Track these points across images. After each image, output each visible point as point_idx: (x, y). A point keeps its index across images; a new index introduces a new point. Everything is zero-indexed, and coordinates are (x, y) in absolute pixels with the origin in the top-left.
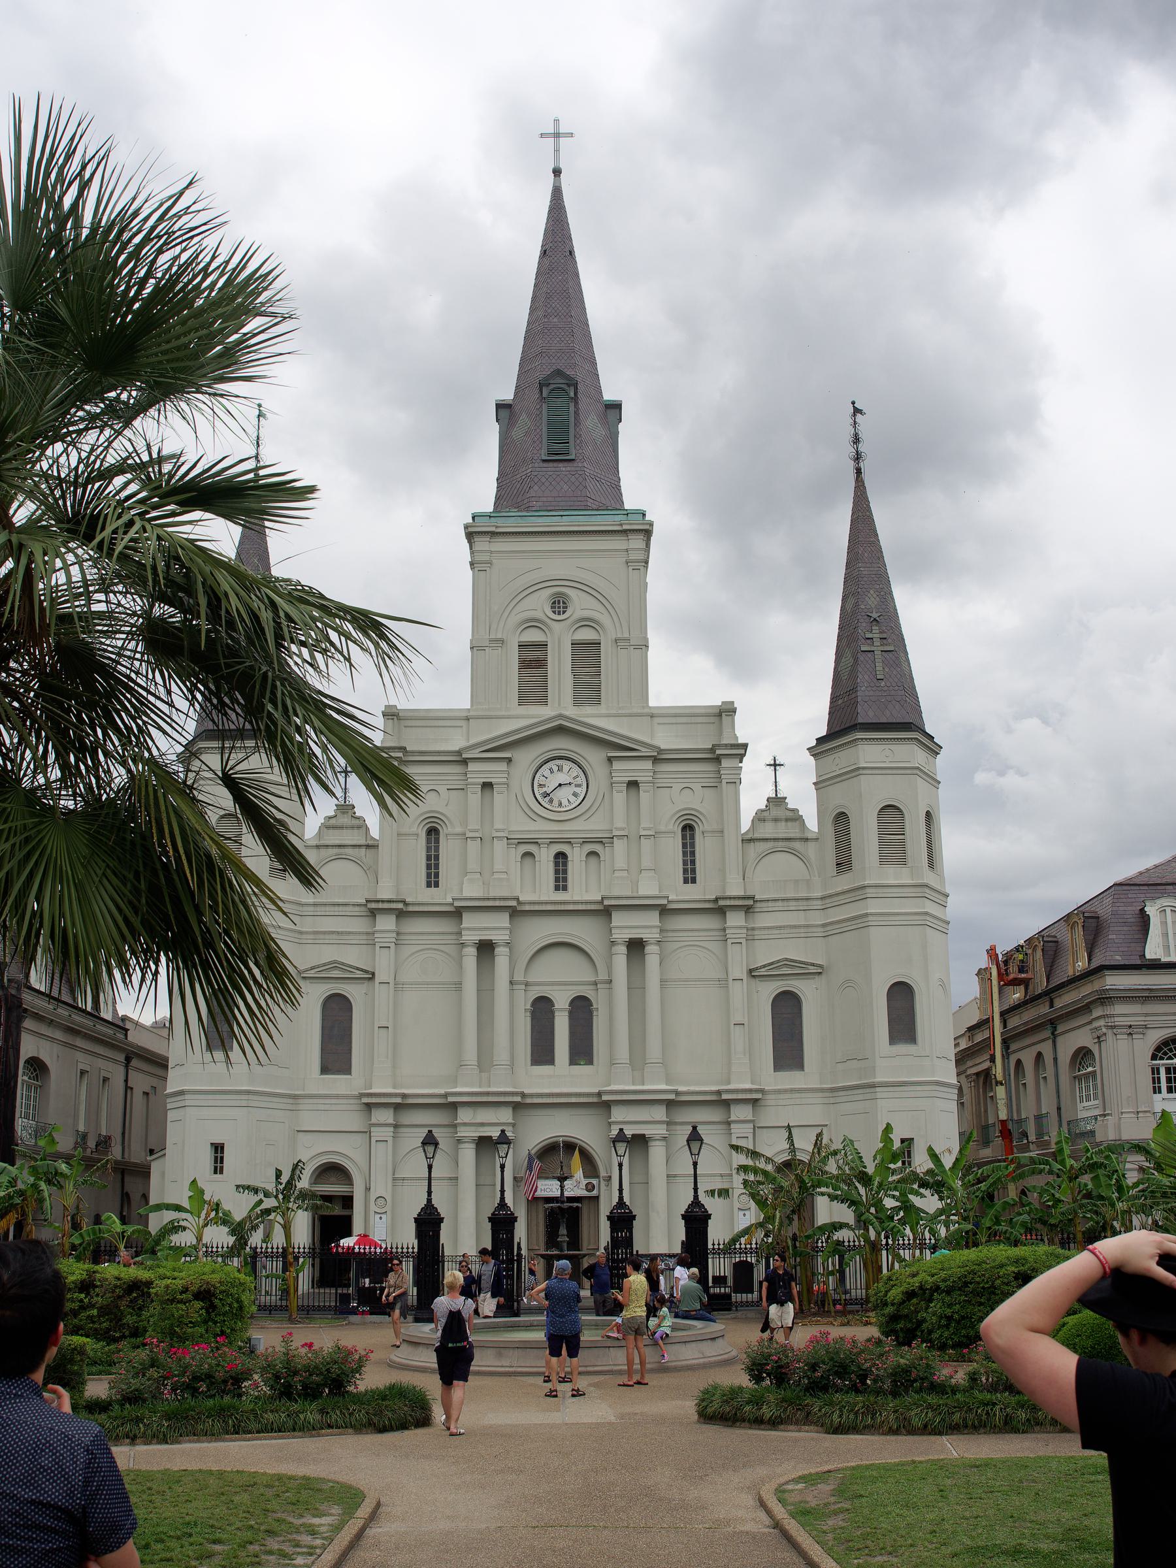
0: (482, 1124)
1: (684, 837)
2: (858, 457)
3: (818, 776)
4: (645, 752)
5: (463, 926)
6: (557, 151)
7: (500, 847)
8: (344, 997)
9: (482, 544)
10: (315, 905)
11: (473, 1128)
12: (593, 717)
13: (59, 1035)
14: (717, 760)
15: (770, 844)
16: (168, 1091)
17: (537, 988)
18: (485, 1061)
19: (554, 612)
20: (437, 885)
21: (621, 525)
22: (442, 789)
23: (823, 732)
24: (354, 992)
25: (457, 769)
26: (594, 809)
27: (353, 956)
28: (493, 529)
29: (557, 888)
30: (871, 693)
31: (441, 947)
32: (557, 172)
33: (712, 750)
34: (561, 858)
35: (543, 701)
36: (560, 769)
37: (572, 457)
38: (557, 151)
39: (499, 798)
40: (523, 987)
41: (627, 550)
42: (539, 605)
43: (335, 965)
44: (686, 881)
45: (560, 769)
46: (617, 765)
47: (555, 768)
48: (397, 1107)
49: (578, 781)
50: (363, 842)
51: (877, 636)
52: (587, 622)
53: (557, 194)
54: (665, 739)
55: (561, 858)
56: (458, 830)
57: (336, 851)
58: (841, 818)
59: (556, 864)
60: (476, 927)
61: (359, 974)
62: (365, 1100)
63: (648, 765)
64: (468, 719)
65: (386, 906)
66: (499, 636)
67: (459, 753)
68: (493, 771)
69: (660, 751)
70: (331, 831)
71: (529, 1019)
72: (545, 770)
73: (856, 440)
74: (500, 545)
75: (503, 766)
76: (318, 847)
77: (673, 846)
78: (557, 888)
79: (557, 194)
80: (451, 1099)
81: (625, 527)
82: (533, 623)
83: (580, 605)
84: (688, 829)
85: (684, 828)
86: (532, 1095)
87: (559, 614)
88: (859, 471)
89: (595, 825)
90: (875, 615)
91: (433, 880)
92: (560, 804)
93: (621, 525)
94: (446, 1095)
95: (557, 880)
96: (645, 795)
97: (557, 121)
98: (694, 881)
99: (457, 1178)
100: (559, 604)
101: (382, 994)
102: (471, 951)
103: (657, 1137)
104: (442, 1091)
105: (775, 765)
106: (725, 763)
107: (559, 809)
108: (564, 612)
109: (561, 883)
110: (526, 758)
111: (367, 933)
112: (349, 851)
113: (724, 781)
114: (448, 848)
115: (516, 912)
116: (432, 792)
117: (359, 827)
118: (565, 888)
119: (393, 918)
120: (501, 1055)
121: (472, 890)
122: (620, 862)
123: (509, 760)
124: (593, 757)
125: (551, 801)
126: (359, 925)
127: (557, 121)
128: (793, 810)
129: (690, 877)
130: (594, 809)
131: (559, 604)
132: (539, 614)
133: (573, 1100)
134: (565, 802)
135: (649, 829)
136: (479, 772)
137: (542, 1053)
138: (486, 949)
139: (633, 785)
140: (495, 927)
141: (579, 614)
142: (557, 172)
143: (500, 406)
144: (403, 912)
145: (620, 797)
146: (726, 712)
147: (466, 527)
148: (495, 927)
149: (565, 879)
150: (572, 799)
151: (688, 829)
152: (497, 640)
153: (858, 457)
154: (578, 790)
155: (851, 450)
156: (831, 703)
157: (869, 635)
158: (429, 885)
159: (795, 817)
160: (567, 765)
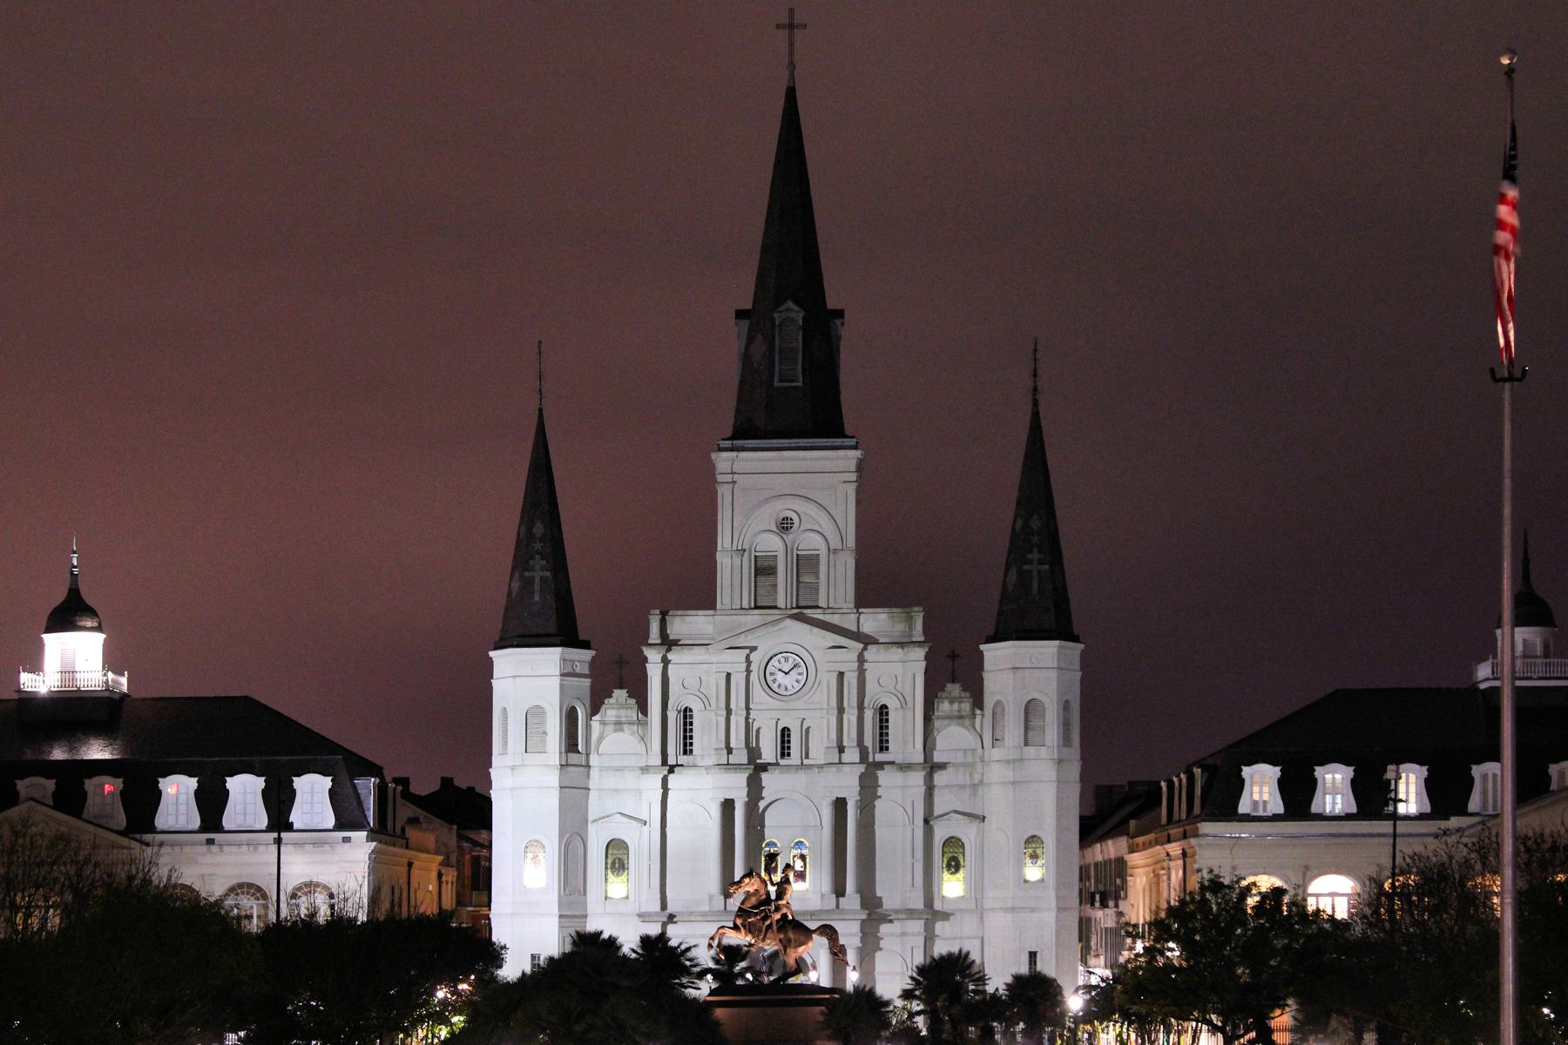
1: (881, 714)
2: (1035, 389)
23: (992, 633)
29: (783, 755)
36: (786, 660)
38: (791, 45)
45: (786, 660)
47: (783, 660)
53: (791, 93)
73: (1035, 375)
79: (791, 93)
92: (786, 689)
118: (789, 755)
134: (789, 687)
143: (741, 314)
150: (796, 685)
153: (1035, 389)
154: (800, 677)
155: (1030, 384)
157: (1029, 556)
158: (685, 753)
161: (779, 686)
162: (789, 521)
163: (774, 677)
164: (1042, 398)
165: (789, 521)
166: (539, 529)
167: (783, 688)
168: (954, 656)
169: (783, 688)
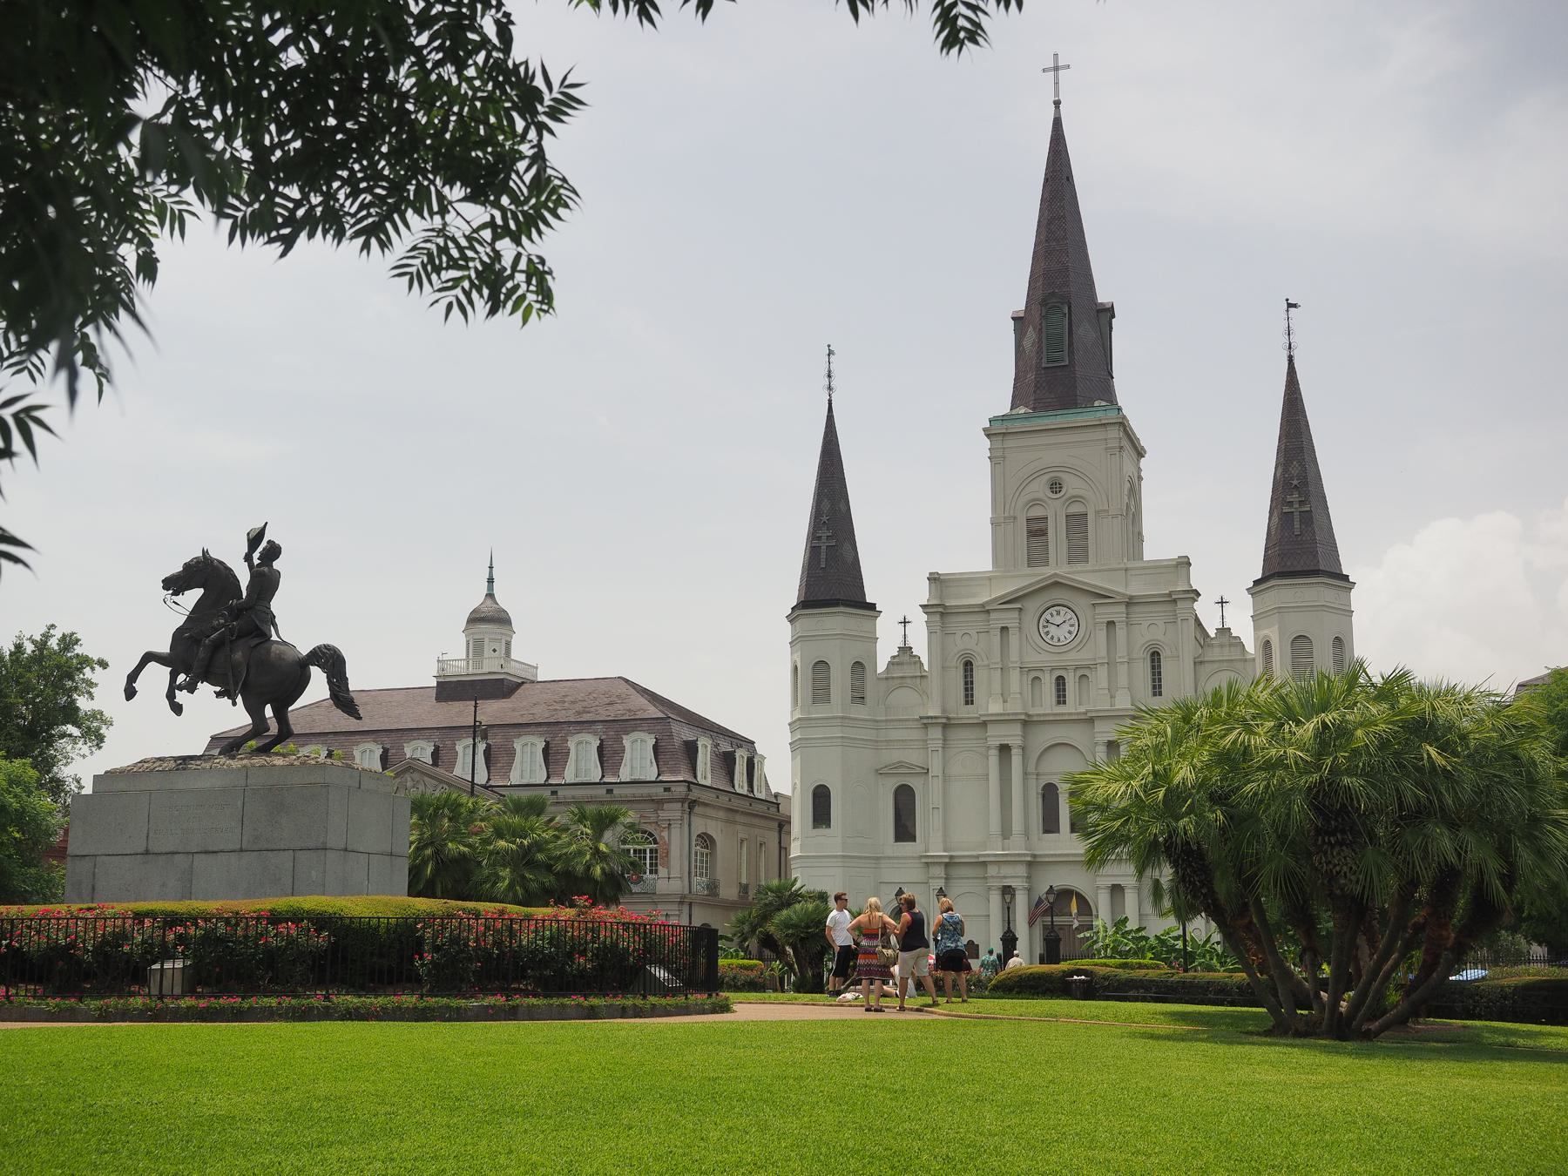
0: (1005, 877)
1: (1153, 661)
2: (1290, 348)
3: (1254, 611)
4: (1119, 599)
5: (988, 734)
6: (1057, 83)
7: (1015, 676)
8: (903, 785)
9: (998, 444)
10: (886, 721)
11: (999, 880)
12: (1084, 575)
13: (721, 814)
14: (1175, 601)
15: (1216, 665)
16: (792, 856)
17: (1044, 777)
18: (1006, 833)
19: (1053, 492)
20: (972, 704)
21: (1100, 420)
22: (973, 633)
23: (1260, 577)
24: (916, 784)
25: (984, 616)
26: (1085, 641)
27: (914, 757)
28: (1004, 431)
29: (1059, 703)
30: (1290, 547)
31: (975, 749)
32: (1057, 104)
33: (1170, 595)
34: (1060, 682)
35: (1046, 563)
36: (1058, 613)
37: (1067, 363)
38: (1057, 83)
39: (1014, 638)
40: (1035, 777)
41: (1106, 440)
42: (1040, 488)
43: (901, 765)
44: (1155, 695)
45: (1058, 613)
46: (1099, 610)
47: (1055, 613)
48: (947, 865)
49: (1072, 622)
50: (919, 674)
51: (1297, 500)
52: (1076, 499)
53: (1057, 123)
54: (1136, 589)
55: (1060, 682)
56: (986, 662)
57: (899, 681)
58: (1267, 645)
59: (1058, 685)
60: (997, 735)
61: (919, 770)
62: (924, 860)
63: (1122, 608)
64: (990, 579)
65: (934, 721)
66: (1012, 514)
67: (983, 605)
68: (1010, 619)
69: (1131, 597)
70: (896, 667)
71: (1040, 800)
72: (1047, 615)
74: (1011, 442)
75: (1015, 614)
76: (887, 679)
77: (1143, 670)
78: (1059, 703)
79: (1057, 123)
80: (981, 859)
81: (1103, 422)
82: (1035, 502)
83: (1072, 486)
84: (1155, 657)
85: (1153, 654)
86: (1040, 856)
87: (1056, 493)
88: (1291, 359)
89: (1084, 656)
90: (1295, 482)
91: (969, 700)
92: (1059, 640)
93: (1100, 420)
94: (978, 856)
95: (1059, 696)
96: (1121, 632)
97: (1056, 55)
98: (1160, 694)
99: (989, 916)
100: (1055, 486)
101: (935, 786)
102: (994, 754)
103: (1129, 886)
104: (974, 853)
105: (1222, 602)
106: (1180, 605)
107: (1058, 644)
108: (1060, 491)
109: (1061, 699)
110: (1033, 606)
111: (923, 740)
112: (909, 681)
113: (1179, 619)
114: (979, 676)
115: (1027, 723)
116: (966, 637)
117: (915, 663)
118: (1064, 702)
119: (940, 729)
120: (1017, 826)
121: (995, 708)
122: (1105, 684)
123: (1021, 609)
124: (1082, 603)
125: (1052, 638)
126: (916, 734)
127: (1056, 55)
128: (1235, 637)
129: (1157, 690)
130: (1085, 641)
131: (1055, 486)
132: (1040, 495)
133: (1071, 859)
134: (1062, 638)
135: (1124, 657)
136: (999, 620)
137: (1050, 825)
138: (1004, 750)
139: (1111, 624)
140: (1013, 736)
141: (1071, 492)
142: (1057, 104)
144: (947, 725)
145: (1102, 634)
146: (1184, 563)
147: (984, 430)
148: (1013, 736)
149: (1064, 696)
150: (1068, 635)
151: (1155, 657)
152: (1010, 517)
153: (1290, 348)
154: (1072, 629)
156: (1265, 552)
157: (1289, 499)
159: (1238, 643)
160: (1063, 610)
161: (1052, 638)
162: (1058, 486)
163: (1047, 629)
164: (1296, 354)
165: (1058, 486)
166: (826, 505)
167: (1056, 639)
168: (1222, 602)
169: (1056, 639)
